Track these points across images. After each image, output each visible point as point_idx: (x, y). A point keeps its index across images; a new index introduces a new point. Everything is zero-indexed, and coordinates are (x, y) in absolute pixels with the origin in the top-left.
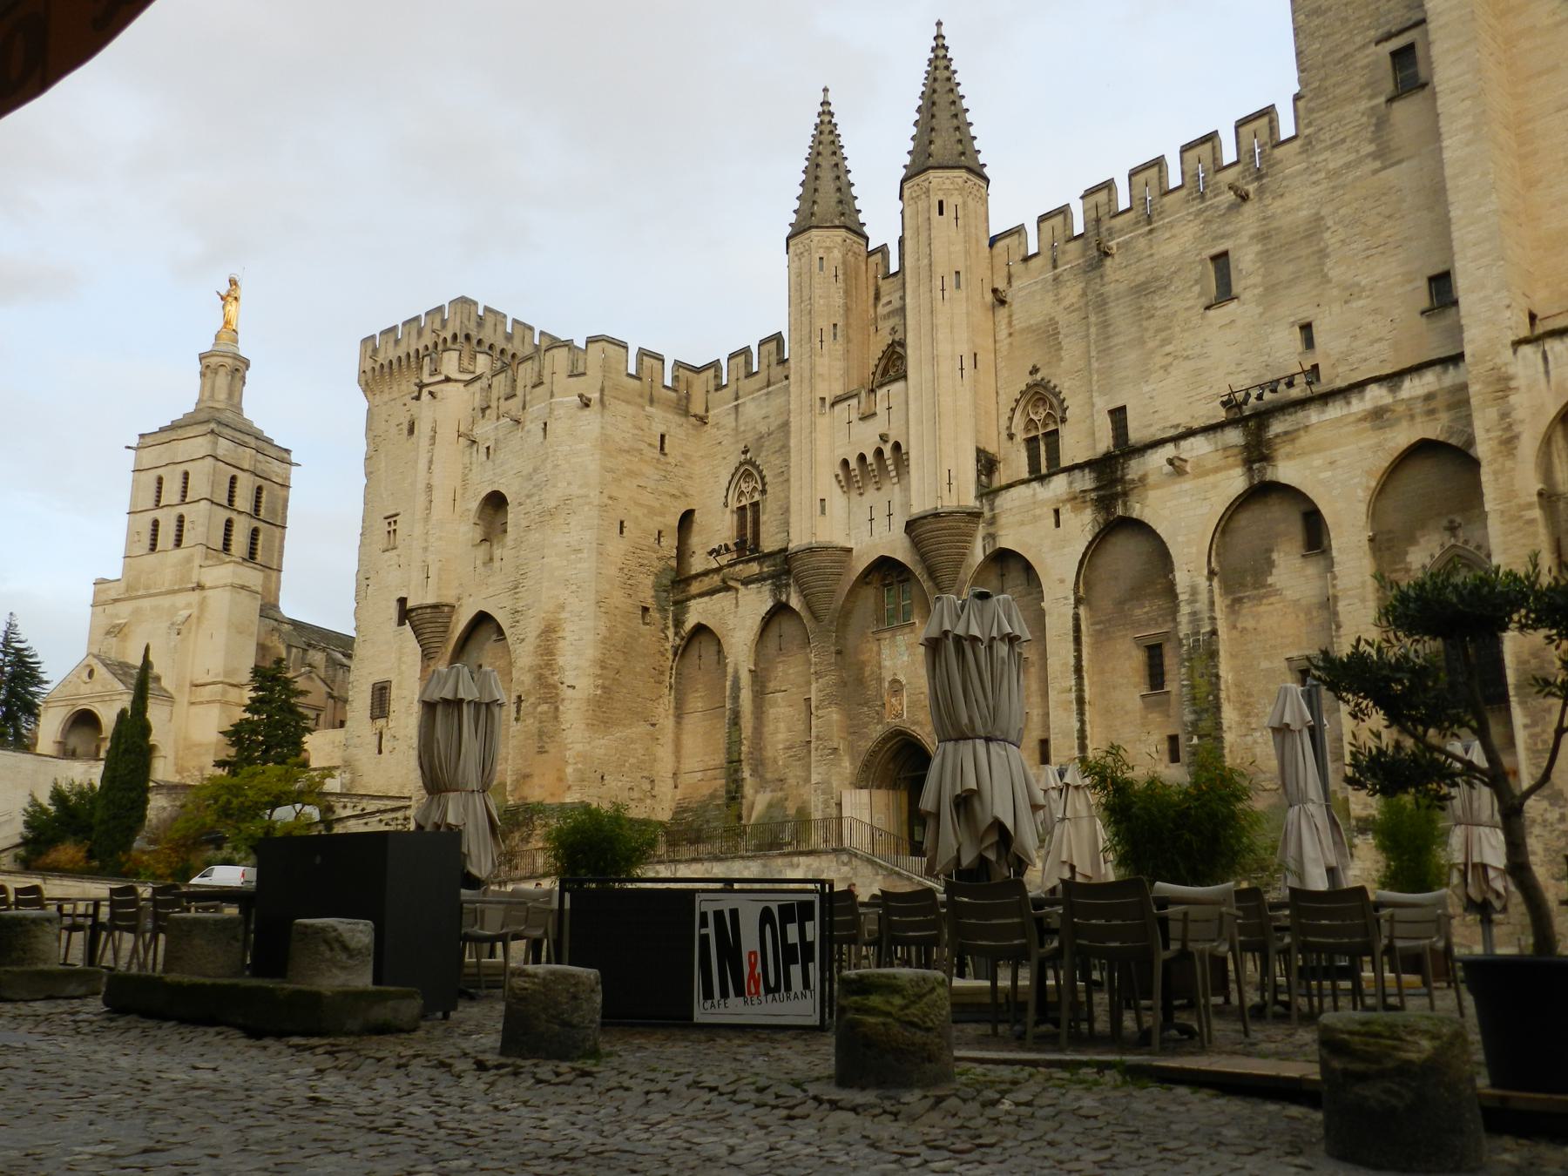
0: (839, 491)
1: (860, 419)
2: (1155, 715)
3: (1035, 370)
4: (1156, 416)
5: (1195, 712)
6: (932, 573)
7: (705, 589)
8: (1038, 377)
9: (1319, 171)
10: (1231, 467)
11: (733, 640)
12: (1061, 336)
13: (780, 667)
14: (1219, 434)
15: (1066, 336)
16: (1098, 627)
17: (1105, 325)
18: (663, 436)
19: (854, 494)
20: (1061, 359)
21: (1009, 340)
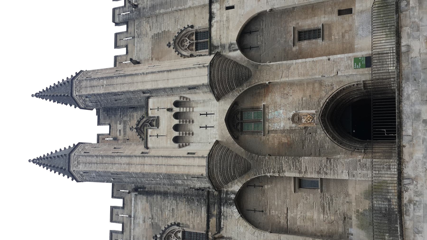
0: (187, 147)
1: (158, 127)
3: (169, 45)
6: (240, 83)
13: (273, 212)
15: (161, 29)
19: (192, 139)
20: (169, 30)
21: (154, 59)
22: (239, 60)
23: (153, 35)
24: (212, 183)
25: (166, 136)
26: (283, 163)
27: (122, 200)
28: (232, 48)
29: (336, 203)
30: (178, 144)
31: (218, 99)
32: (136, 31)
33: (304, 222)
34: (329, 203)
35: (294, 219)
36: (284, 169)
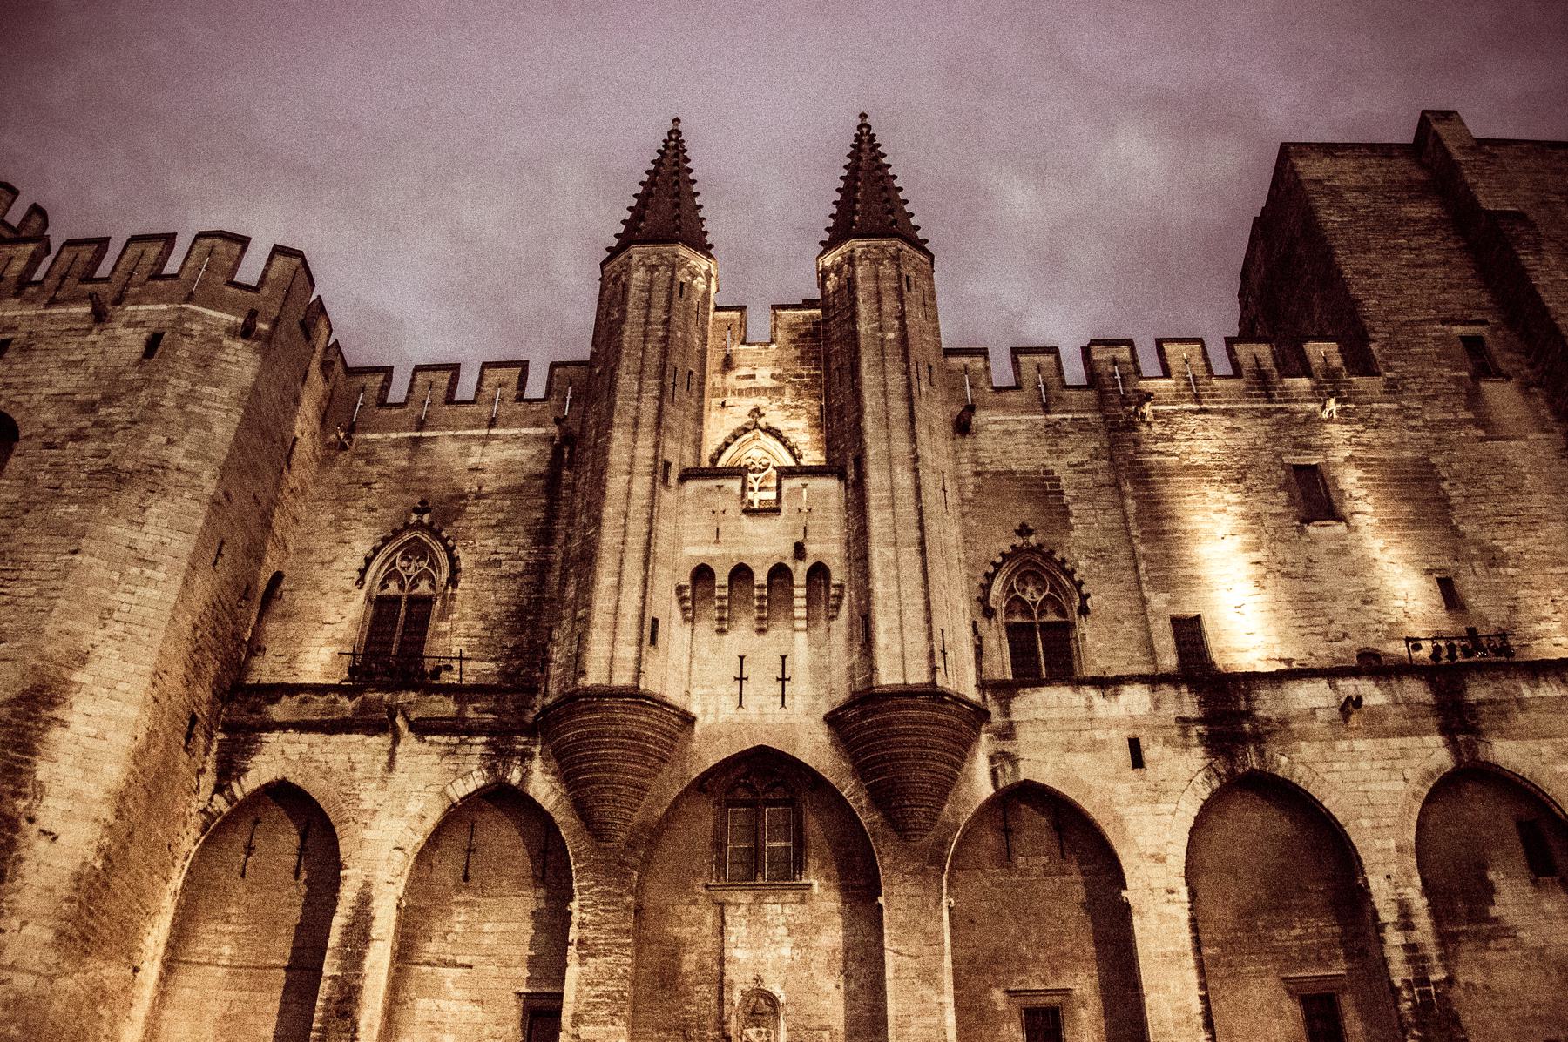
0: (677, 615)
3: (1024, 531)
6: (882, 797)
8: (1032, 540)
9: (1414, 418)
10: (1427, 733)
11: (368, 834)
12: (1066, 499)
15: (1075, 499)
19: (705, 628)
20: (1071, 528)
22: (964, 789)
23: (1056, 474)
24: (556, 704)
25: (717, 542)
26: (608, 959)
27: (542, 396)
28: (1002, 767)
30: (688, 583)
31: (832, 720)
32: (1065, 416)
36: (590, 960)
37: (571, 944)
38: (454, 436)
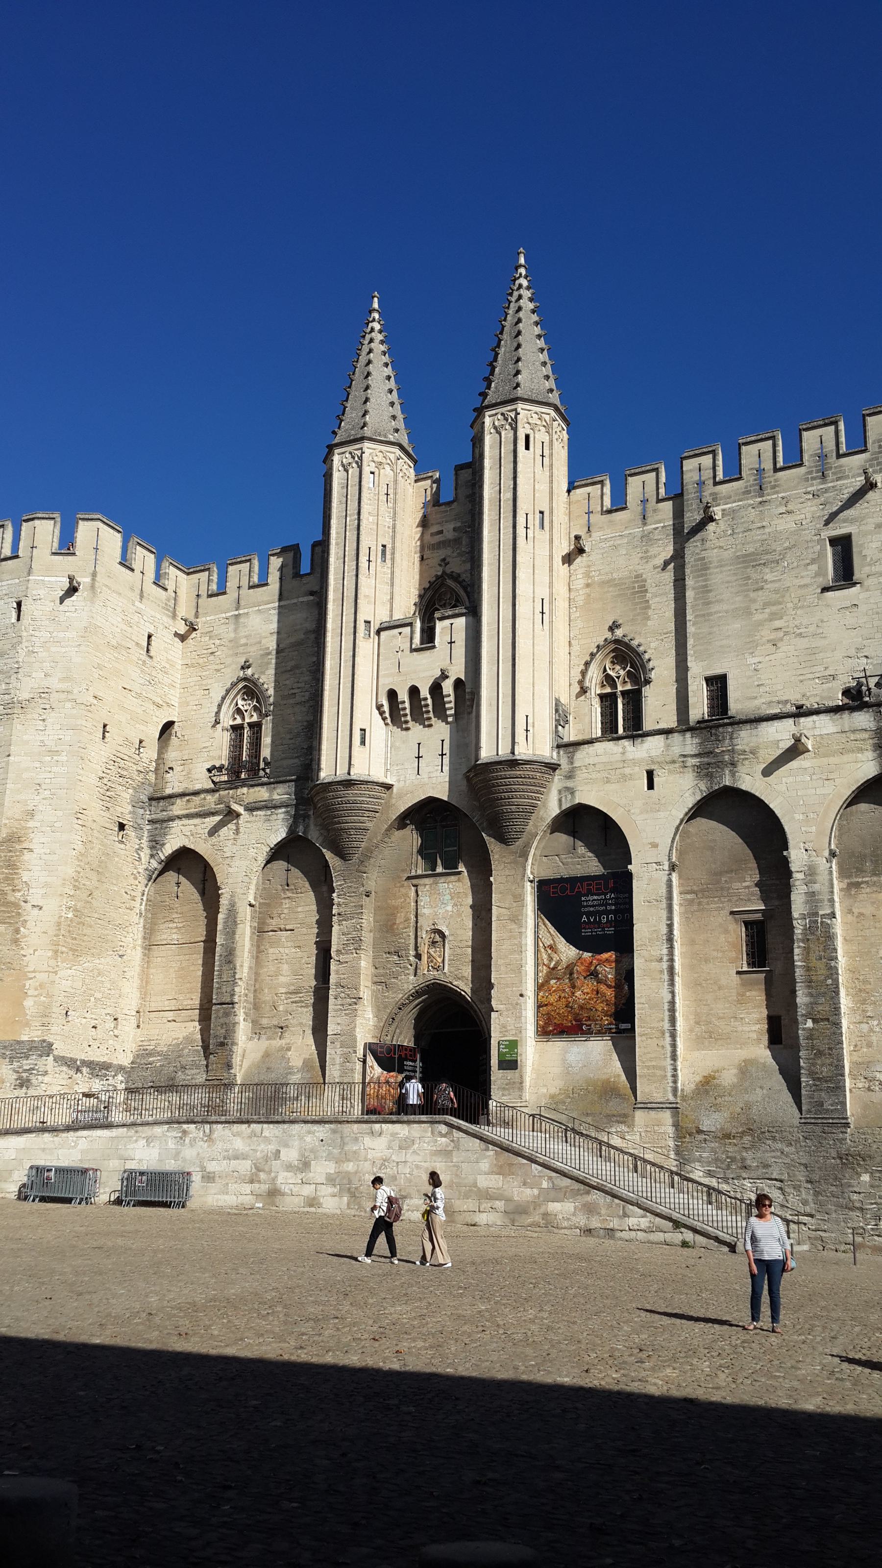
2: (754, 993)
4: (762, 689)
5: (811, 995)
7: (193, 811)
8: (619, 633)
11: (231, 870)
13: (286, 904)
14: (846, 715)
16: (689, 896)
17: (705, 590)
18: (150, 637)
20: (648, 618)
21: (588, 590)
22: (541, 813)
29: (302, 1013)
33: (273, 960)
34: (302, 1002)
35: (276, 944)
36: (344, 922)
37: (335, 916)
38: (259, 610)
